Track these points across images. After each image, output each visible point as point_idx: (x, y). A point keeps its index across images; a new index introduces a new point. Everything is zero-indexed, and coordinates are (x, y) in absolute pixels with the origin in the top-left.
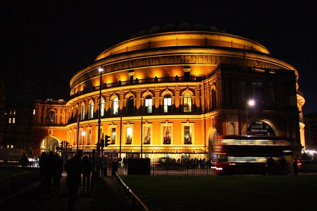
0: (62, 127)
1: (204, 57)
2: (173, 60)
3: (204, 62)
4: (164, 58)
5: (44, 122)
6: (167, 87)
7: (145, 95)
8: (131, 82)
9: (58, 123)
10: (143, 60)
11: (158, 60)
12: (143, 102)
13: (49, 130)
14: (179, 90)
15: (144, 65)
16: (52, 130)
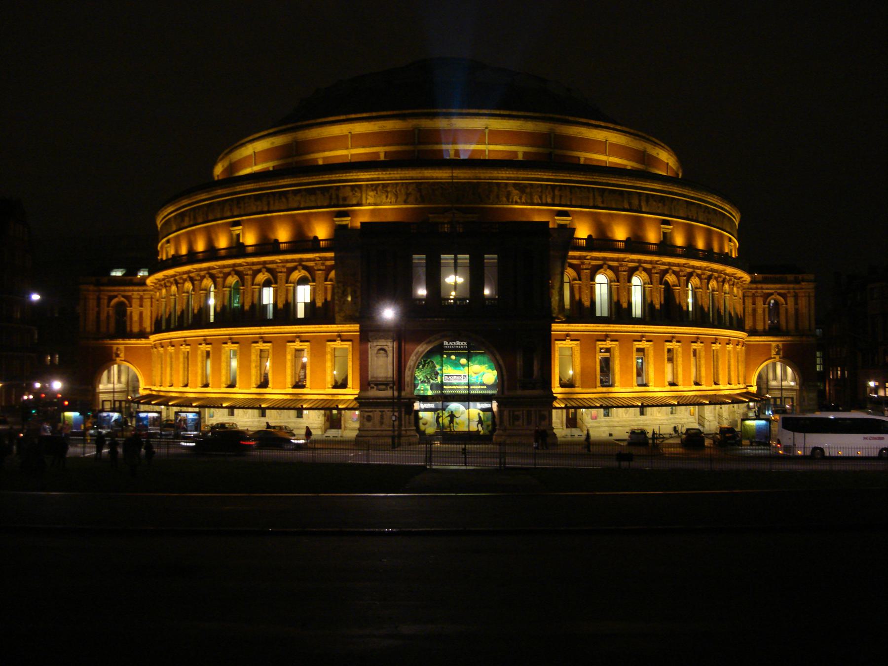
0: (143, 341)
1: (380, 187)
2: (313, 198)
3: (378, 201)
4: (295, 193)
5: (103, 329)
6: (301, 260)
7: (262, 277)
8: (237, 249)
9: (136, 329)
10: (258, 198)
11: (284, 200)
12: (256, 295)
13: (115, 347)
14: (323, 267)
15: (259, 209)
16: (122, 347)
